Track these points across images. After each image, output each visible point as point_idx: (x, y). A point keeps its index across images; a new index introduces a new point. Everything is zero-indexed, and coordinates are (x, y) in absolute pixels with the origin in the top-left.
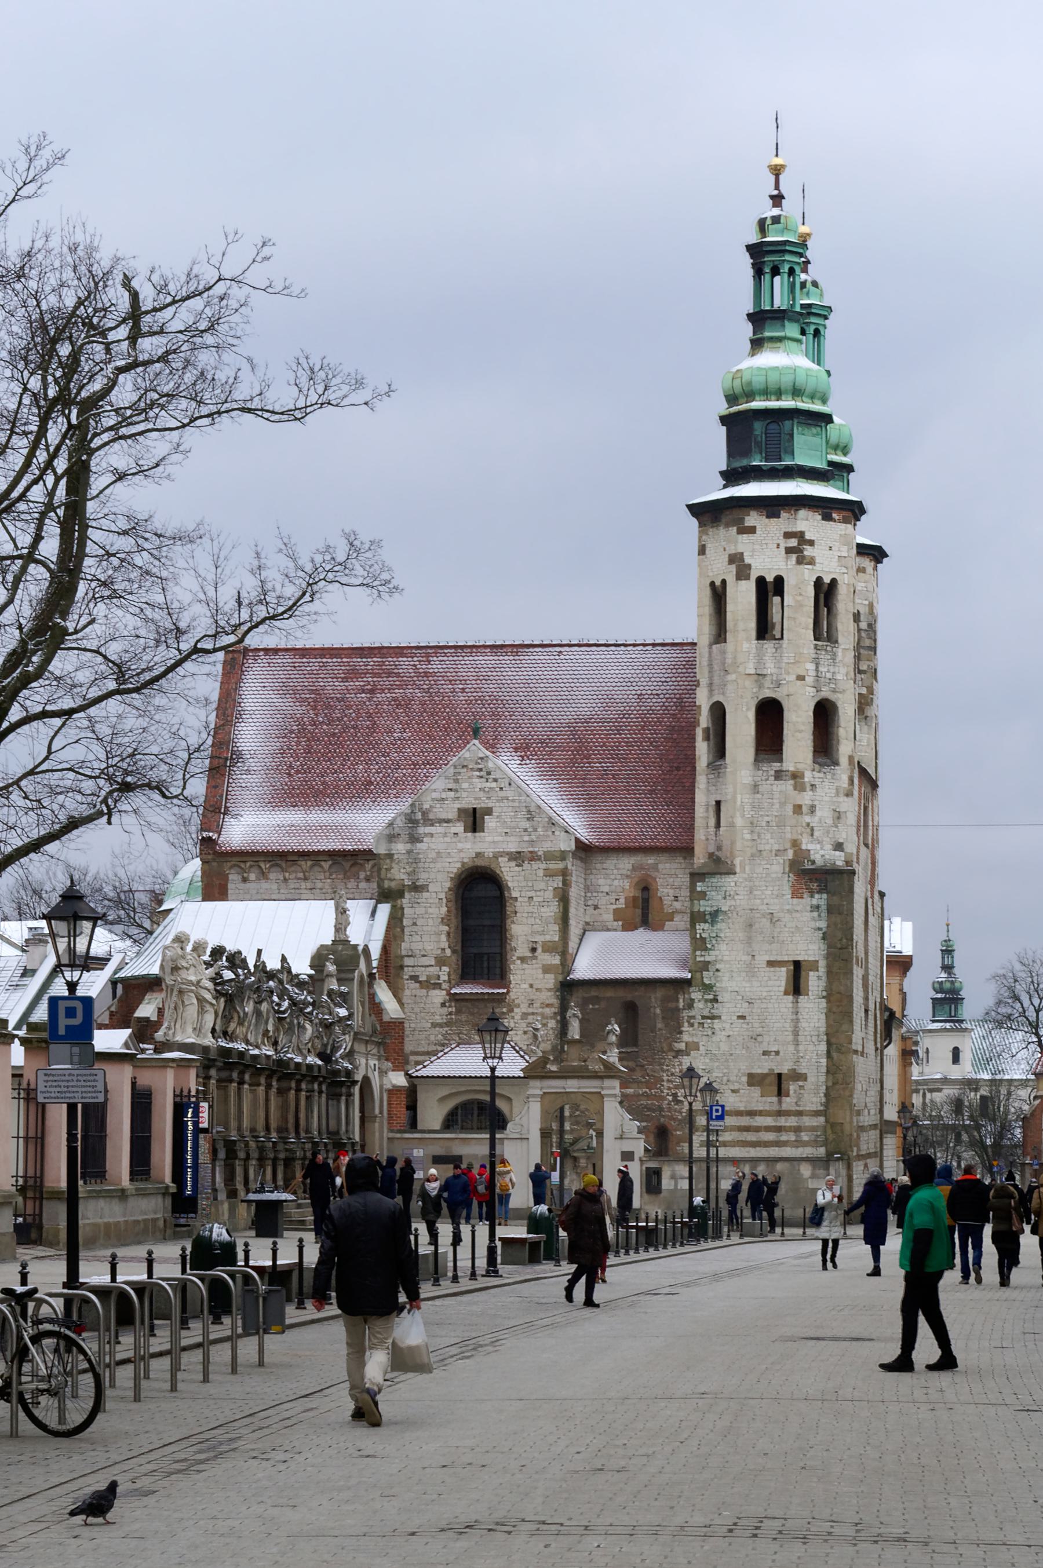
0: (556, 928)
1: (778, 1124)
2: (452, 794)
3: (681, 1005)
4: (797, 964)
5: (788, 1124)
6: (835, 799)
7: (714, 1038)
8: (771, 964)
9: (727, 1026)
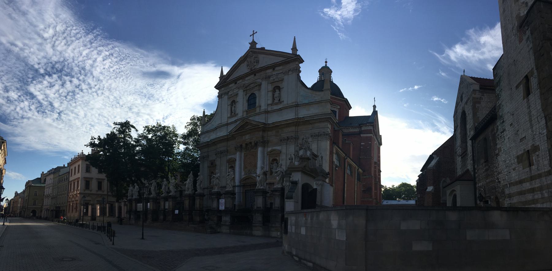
1: (532, 187)
4: (526, 77)
5: (536, 186)
7: (505, 142)
9: (509, 133)
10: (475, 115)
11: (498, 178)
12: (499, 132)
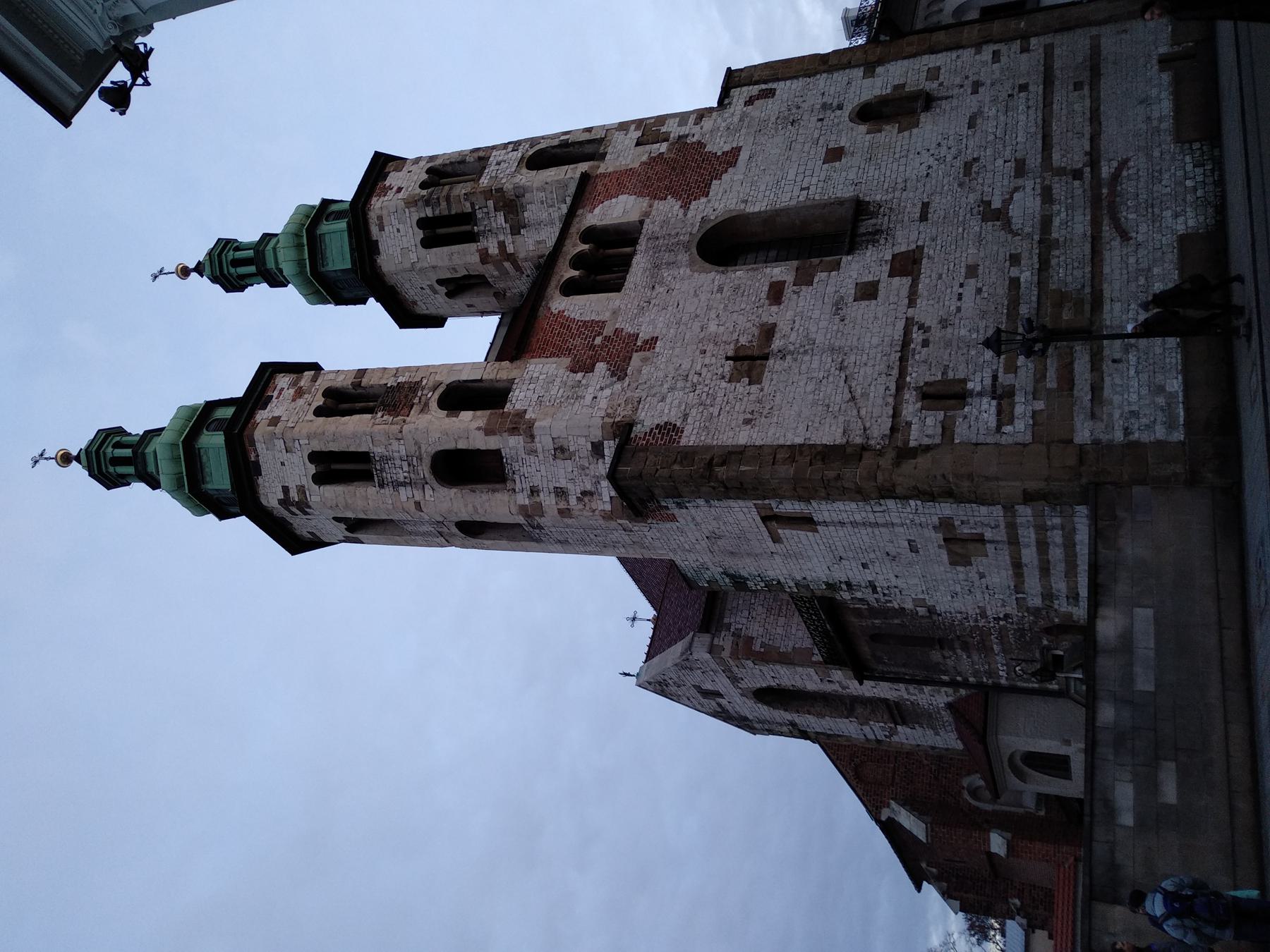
0: (800, 669)
1: (1034, 543)
2: (691, 699)
3: (861, 606)
4: (765, 519)
5: (1033, 536)
6: (541, 456)
8: (776, 539)
9: (883, 575)
10: (785, 659)
11: (994, 618)
12: (871, 598)
